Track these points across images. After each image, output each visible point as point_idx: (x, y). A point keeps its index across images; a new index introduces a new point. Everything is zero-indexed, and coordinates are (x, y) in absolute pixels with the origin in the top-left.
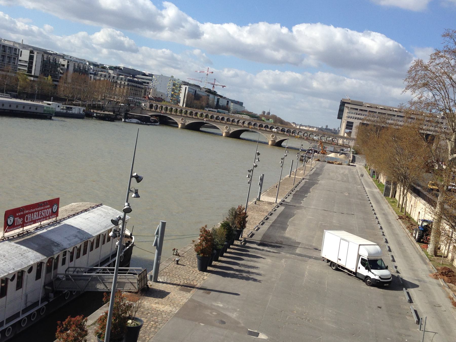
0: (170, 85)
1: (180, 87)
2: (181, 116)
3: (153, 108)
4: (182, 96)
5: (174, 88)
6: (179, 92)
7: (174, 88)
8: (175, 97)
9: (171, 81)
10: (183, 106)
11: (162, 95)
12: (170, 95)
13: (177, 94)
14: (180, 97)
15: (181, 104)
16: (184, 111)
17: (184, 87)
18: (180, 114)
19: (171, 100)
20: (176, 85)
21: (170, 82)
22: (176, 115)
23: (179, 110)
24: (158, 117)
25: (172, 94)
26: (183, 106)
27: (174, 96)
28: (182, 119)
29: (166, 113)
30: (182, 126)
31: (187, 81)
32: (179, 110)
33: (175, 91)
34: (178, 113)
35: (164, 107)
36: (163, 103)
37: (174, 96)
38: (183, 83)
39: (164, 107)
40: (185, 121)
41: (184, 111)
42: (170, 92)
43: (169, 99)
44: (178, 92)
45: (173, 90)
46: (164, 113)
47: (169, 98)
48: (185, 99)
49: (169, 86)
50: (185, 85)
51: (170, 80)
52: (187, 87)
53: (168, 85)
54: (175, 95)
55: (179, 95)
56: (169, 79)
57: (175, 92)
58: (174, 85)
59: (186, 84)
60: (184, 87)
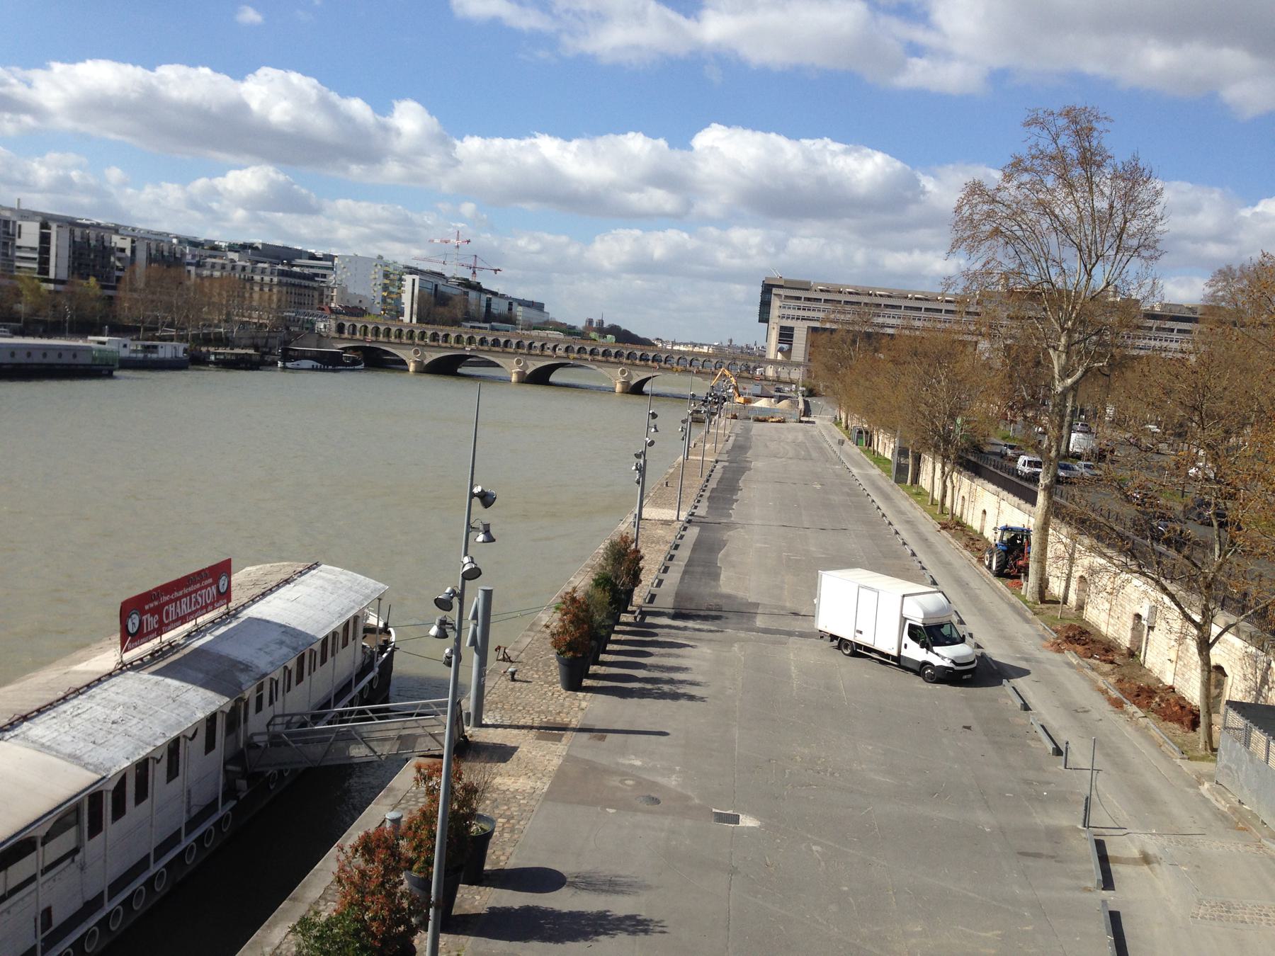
0: (377, 276)
1: (401, 280)
2: (413, 344)
3: (346, 331)
4: (406, 299)
5: (387, 282)
6: (399, 291)
7: (387, 282)
8: (390, 304)
9: (379, 267)
10: (411, 321)
11: (360, 301)
12: (378, 300)
13: (394, 296)
14: (403, 301)
15: (406, 319)
16: (417, 332)
17: (408, 279)
18: (410, 342)
19: (383, 310)
20: (392, 276)
21: (377, 270)
22: (401, 344)
23: (405, 331)
24: (360, 352)
25: (383, 296)
26: (411, 321)
27: (389, 301)
28: (416, 352)
29: (377, 341)
30: (416, 367)
31: (414, 264)
32: (405, 331)
33: (391, 289)
34: (405, 338)
35: (370, 327)
36: (366, 319)
37: (389, 301)
38: (406, 270)
39: (370, 327)
40: (423, 356)
41: (417, 332)
42: (379, 294)
43: (377, 308)
44: (395, 290)
45: (385, 288)
46: (372, 342)
47: (378, 306)
48: (415, 306)
49: (375, 279)
50: (411, 274)
51: (376, 266)
52: (417, 278)
53: (373, 276)
54: (392, 299)
55: (401, 296)
56: (374, 264)
57: (390, 293)
58: (386, 275)
59: (413, 271)
60: (408, 279)
